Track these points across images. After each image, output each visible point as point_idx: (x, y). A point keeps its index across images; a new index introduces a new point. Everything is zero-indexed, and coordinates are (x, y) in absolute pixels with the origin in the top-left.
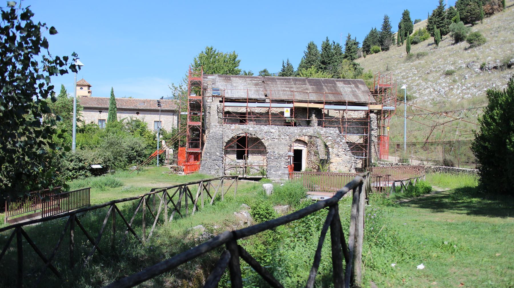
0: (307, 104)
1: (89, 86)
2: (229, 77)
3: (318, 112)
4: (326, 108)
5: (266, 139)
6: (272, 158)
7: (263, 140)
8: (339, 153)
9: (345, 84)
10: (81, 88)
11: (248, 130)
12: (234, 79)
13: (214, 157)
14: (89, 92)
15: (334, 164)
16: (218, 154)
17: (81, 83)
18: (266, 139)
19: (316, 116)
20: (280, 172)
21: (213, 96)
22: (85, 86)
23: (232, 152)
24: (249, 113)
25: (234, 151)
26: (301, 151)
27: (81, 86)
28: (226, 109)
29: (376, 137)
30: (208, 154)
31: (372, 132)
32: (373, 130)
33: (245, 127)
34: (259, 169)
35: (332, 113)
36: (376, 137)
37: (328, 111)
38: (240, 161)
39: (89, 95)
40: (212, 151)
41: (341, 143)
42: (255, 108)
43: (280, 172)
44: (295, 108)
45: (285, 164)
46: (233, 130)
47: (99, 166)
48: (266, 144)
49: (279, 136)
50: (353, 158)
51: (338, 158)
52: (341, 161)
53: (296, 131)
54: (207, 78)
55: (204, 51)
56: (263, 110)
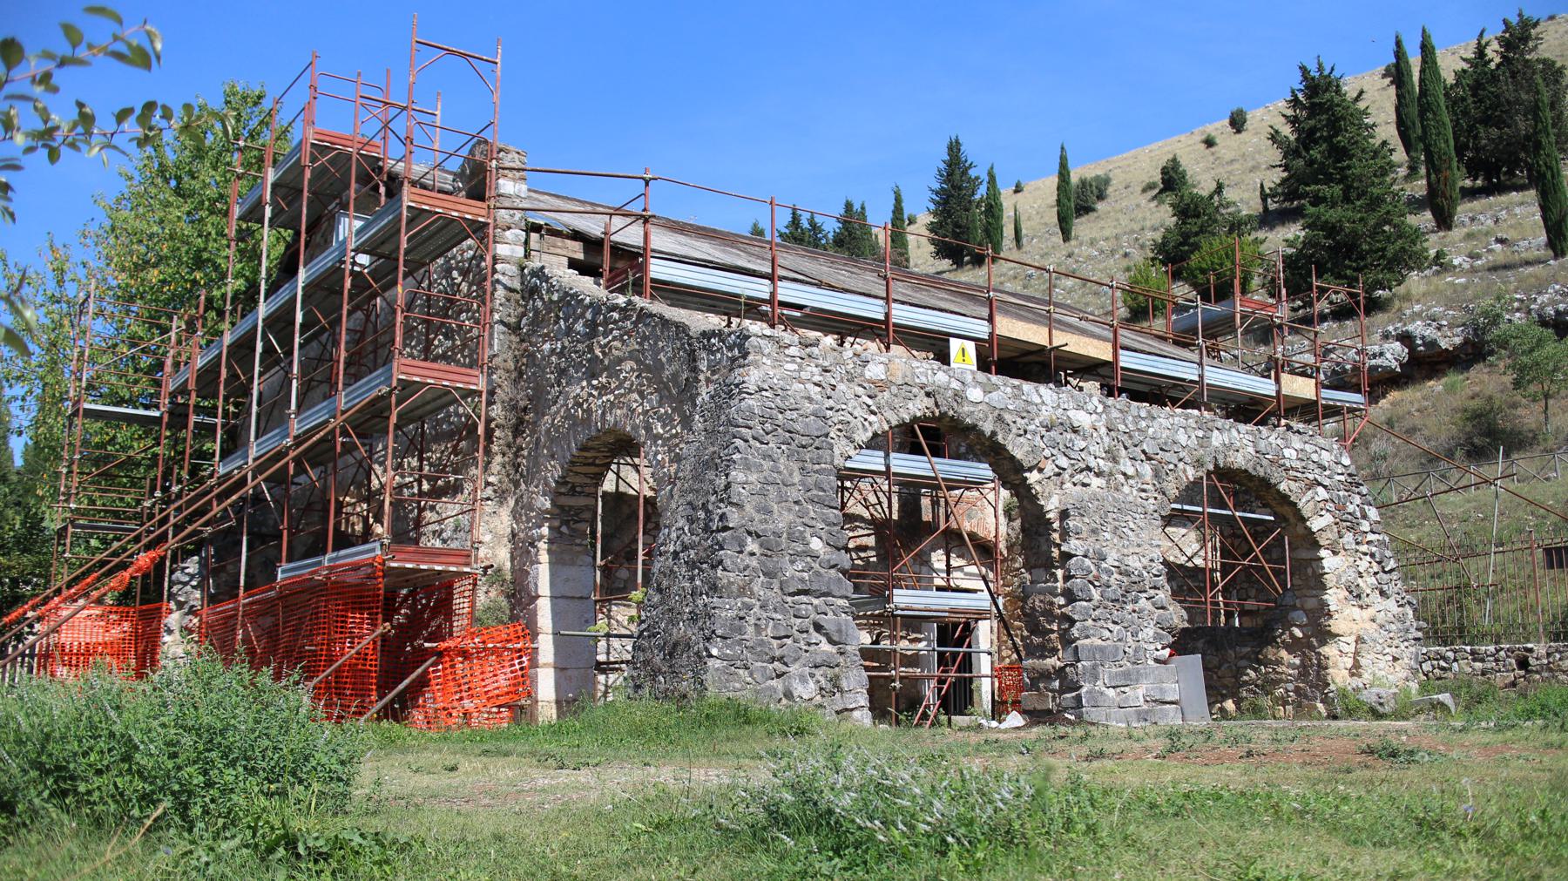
5: (1050, 468)
16: (816, 544)
18: (1050, 468)
20: (1141, 692)
30: (752, 545)
46: (881, 385)
53: (1182, 438)
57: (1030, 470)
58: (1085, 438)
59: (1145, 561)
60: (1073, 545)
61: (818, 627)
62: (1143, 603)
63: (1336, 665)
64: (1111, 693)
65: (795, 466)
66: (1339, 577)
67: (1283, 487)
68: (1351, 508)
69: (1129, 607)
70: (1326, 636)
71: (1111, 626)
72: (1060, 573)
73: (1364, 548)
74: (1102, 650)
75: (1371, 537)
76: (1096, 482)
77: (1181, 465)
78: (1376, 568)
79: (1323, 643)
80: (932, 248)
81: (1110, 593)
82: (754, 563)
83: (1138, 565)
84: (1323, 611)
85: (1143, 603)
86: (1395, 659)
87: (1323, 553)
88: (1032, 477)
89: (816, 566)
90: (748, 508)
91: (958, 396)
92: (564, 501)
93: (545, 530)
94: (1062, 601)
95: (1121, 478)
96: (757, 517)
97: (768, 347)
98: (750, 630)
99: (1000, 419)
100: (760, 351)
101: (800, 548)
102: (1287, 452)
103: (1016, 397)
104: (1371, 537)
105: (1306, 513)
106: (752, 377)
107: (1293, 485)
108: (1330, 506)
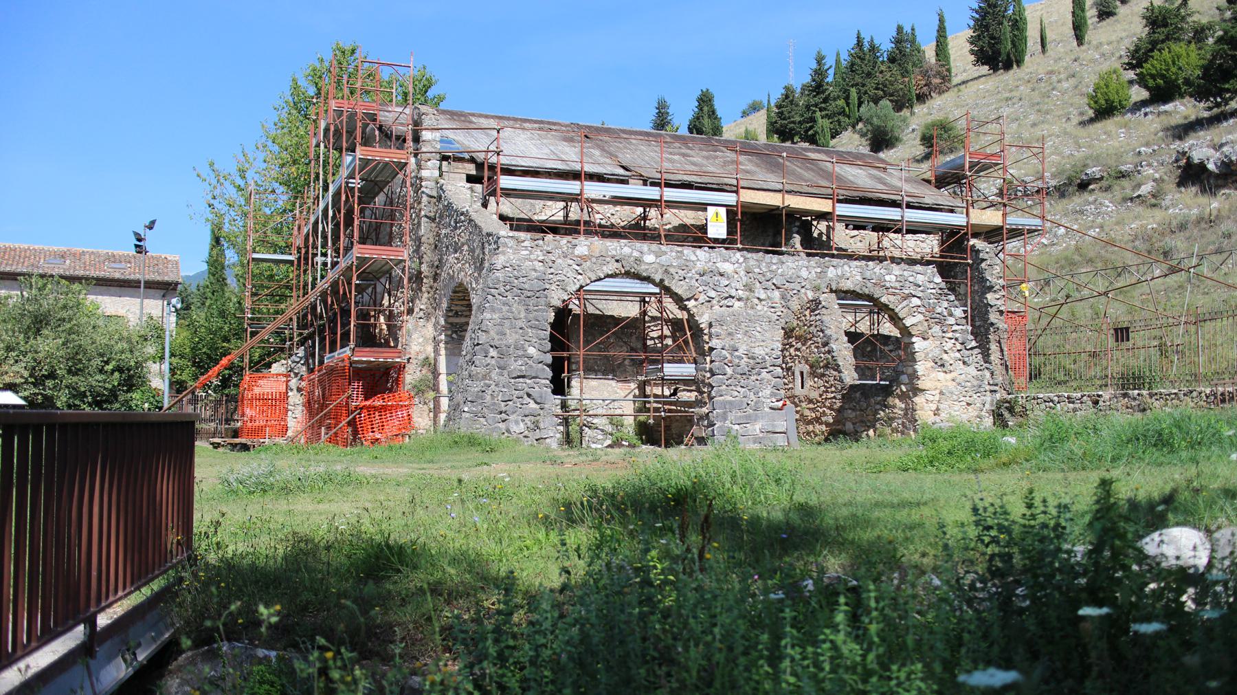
0: (779, 196)
5: (702, 298)
6: (729, 371)
8: (945, 356)
11: (638, 261)
13: (516, 366)
16: (532, 351)
18: (702, 298)
20: (758, 427)
30: (493, 352)
31: (989, 296)
32: (990, 289)
33: (627, 250)
34: (609, 428)
41: (951, 321)
43: (758, 427)
44: (746, 206)
46: (584, 258)
49: (749, 288)
51: (941, 375)
53: (804, 273)
55: (328, 56)
57: (689, 299)
58: (728, 278)
60: (714, 343)
61: (529, 395)
62: (764, 374)
63: (922, 409)
65: (522, 308)
66: (927, 354)
67: (882, 300)
68: (939, 310)
69: (753, 378)
70: (917, 391)
71: (739, 389)
72: (708, 359)
73: (950, 335)
74: (731, 403)
75: (955, 327)
76: (737, 304)
77: (803, 290)
78: (959, 347)
79: (915, 395)
80: (973, 58)
81: (739, 370)
82: (493, 362)
83: (762, 352)
84: (914, 376)
85: (764, 374)
86: (969, 404)
87: (914, 339)
88: (690, 304)
89: (530, 362)
90: (492, 333)
91: (638, 261)
92: (451, 320)
93: (443, 337)
94: (708, 375)
95: (756, 301)
96: (496, 337)
97: (511, 243)
98: (488, 398)
99: (666, 271)
100: (505, 245)
101: (521, 352)
102: (887, 278)
103: (678, 258)
104: (955, 327)
105: (901, 315)
106: (500, 260)
107: (892, 298)
108: (922, 309)
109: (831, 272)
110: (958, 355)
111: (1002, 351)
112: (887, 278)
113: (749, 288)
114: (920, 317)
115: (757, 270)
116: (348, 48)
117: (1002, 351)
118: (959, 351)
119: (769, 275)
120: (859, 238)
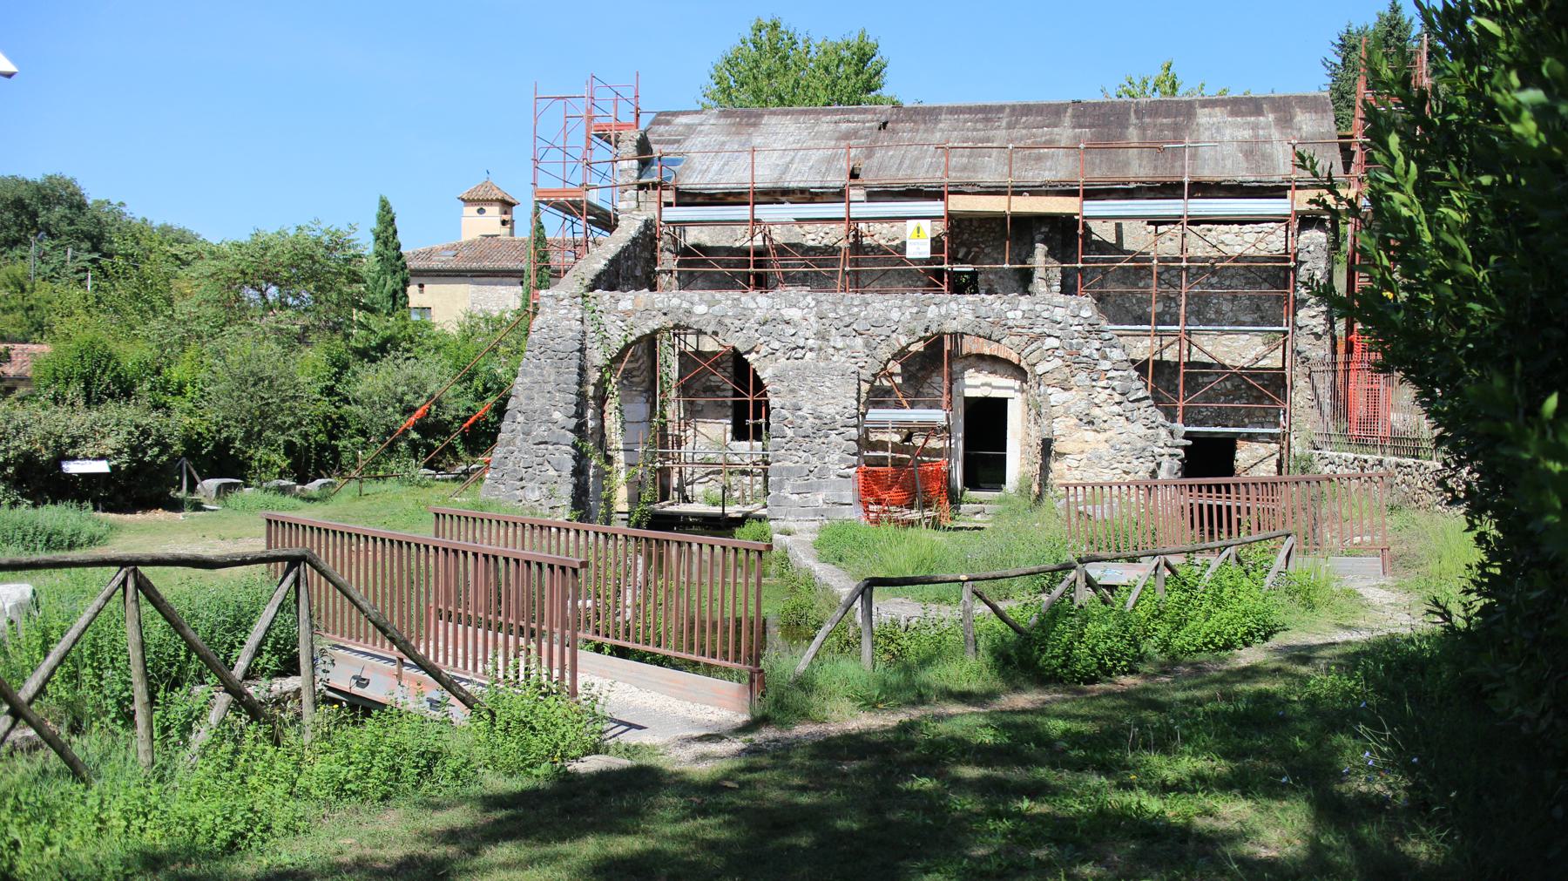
0: (1004, 199)
1: (507, 205)
2: (761, 116)
3: (1064, 235)
4: (1100, 217)
5: (764, 350)
6: (790, 433)
7: (750, 358)
8: (1096, 412)
9: (1233, 114)
10: (481, 211)
12: (774, 120)
13: (540, 432)
14: (504, 223)
15: (1069, 461)
16: (557, 415)
17: (481, 194)
18: (764, 350)
19: (1051, 253)
20: (820, 497)
21: (641, 187)
22: (490, 202)
23: (716, 411)
24: (782, 250)
25: (722, 405)
26: (1002, 404)
27: (479, 202)
28: (693, 236)
29: (1318, 336)
30: (520, 418)
33: (675, 302)
35: (1137, 238)
36: (1318, 336)
37: (1119, 226)
38: (744, 446)
39: (506, 230)
40: (537, 405)
41: (1106, 365)
42: (781, 222)
43: (820, 497)
45: (842, 460)
46: (627, 313)
47: (103, 467)
48: (765, 375)
50: (1163, 433)
51: (1090, 435)
52: (1104, 449)
54: (668, 123)
55: (748, 34)
56: (835, 235)
57: (748, 352)
58: (795, 326)
59: (839, 409)
64: (795, 497)
65: (553, 371)
68: (1086, 352)
71: (801, 453)
73: (1104, 383)
74: (788, 469)
76: (809, 355)
78: (1117, 398)
83: (832, 411)
91: (689, 312)
95: (831, 351)
99: (720, 323)
100: (544, 304)
101: (545, 418)
102: (1010, 315)
103: (734, 306)
109: (932, 312)
110: (1117, 409)
111: (1314, 388)
112: (1010, 315)
113: (822, 336)
114: (1058, 362)
115: (832, 315)
116: (767, 21)
117: (1314, 388)
118: (1119, 403)
119: (847, 320)
120: (1168, 236)
